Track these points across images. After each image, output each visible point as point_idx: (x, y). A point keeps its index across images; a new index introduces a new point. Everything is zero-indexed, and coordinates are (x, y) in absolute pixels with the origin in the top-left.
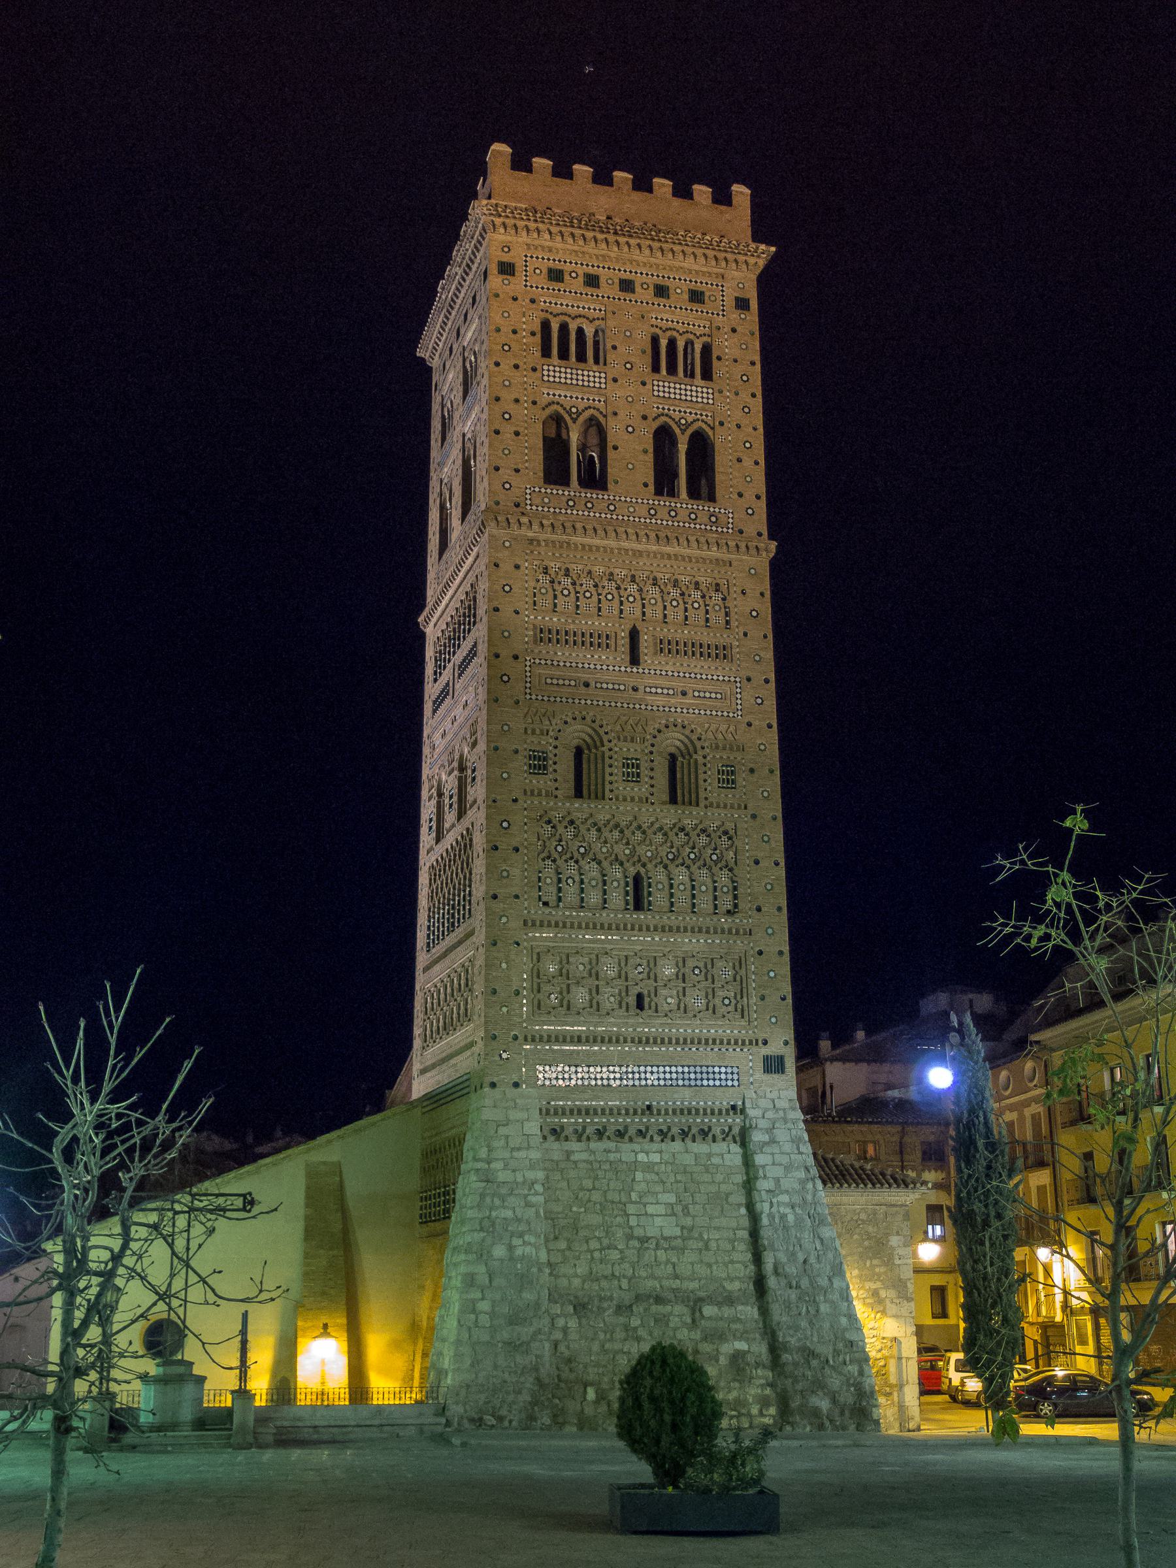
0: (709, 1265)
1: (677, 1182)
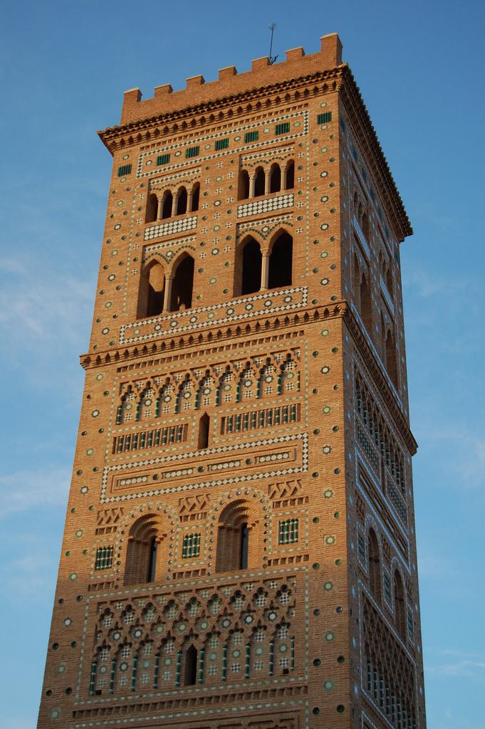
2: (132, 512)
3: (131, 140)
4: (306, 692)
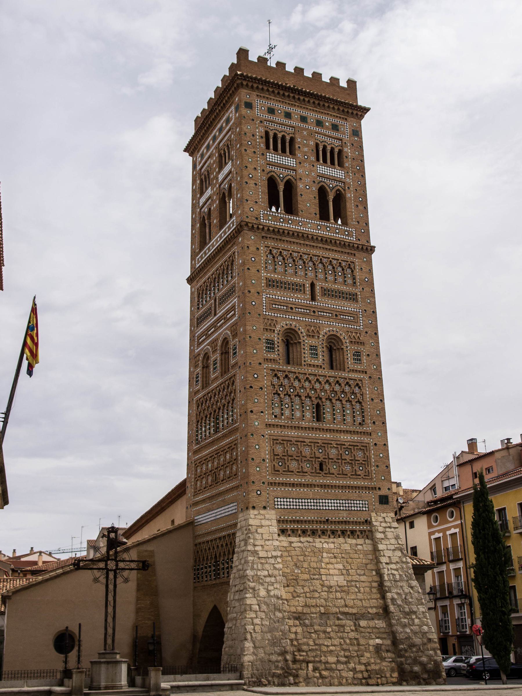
0: (361, 600)
1: (343, 558)
3: (252, 87)
4: (371, 435)
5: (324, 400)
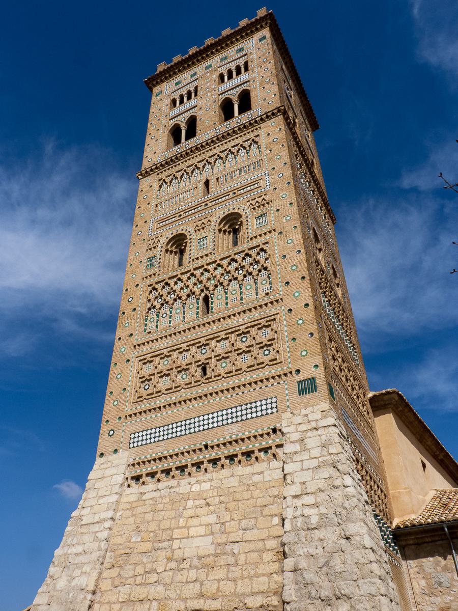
2: (167, 236)
5: (211, 288)
